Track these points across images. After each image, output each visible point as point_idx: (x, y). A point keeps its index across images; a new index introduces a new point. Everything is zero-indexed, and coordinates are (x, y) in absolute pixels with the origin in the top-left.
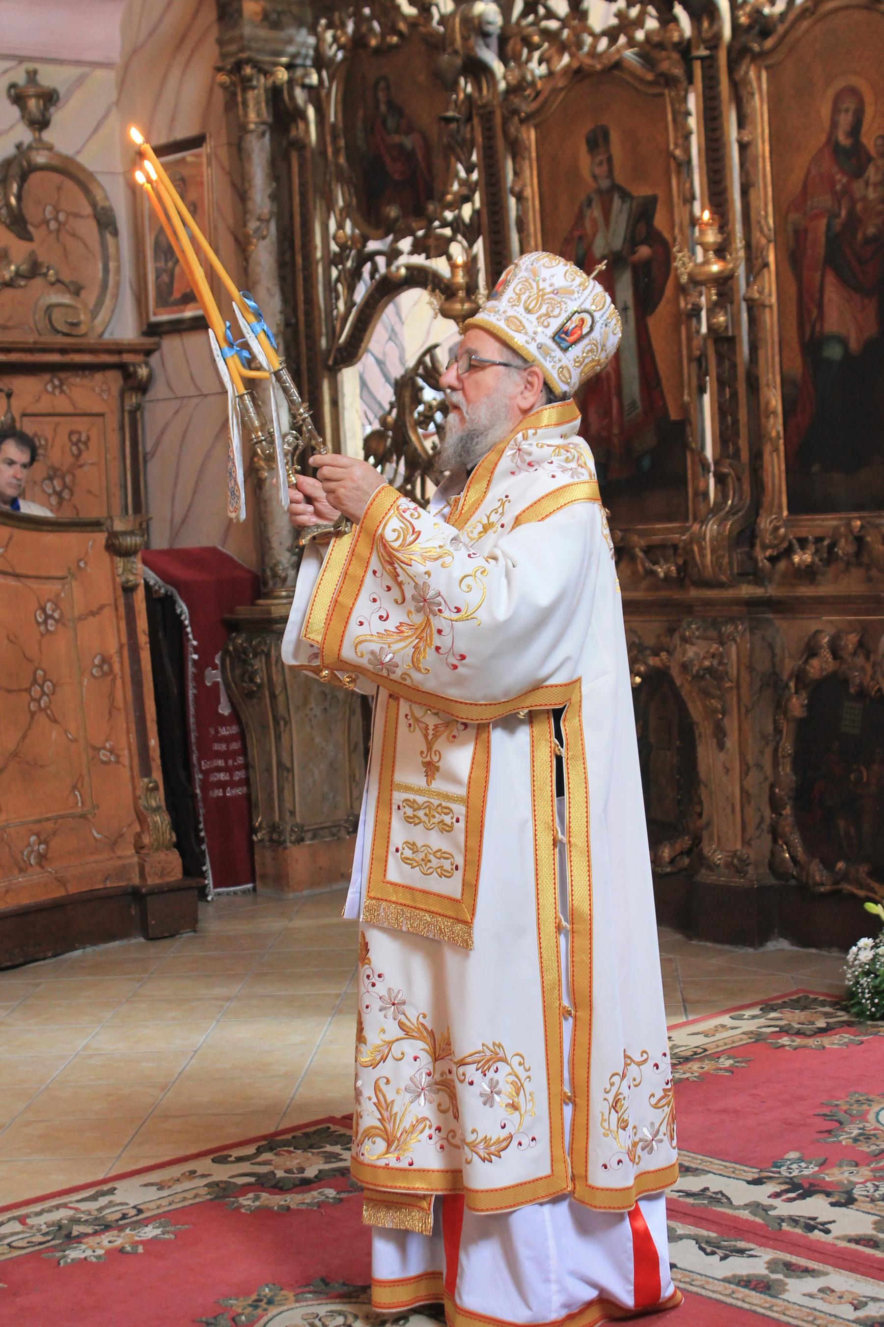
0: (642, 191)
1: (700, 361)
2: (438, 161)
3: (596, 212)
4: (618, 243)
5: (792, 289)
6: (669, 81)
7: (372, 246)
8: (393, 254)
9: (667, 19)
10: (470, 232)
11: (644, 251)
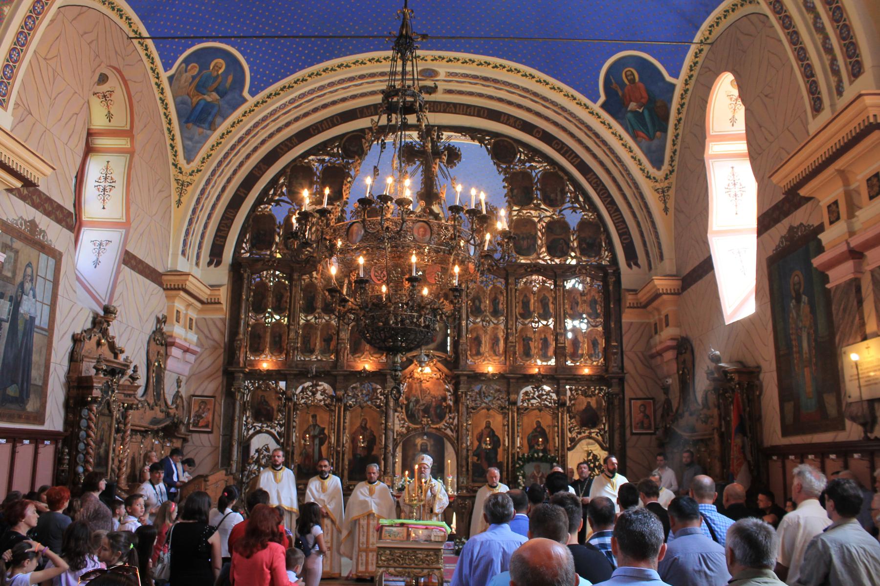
0: (323, 426)
1: (333, 455)
2: (275, 413)
3: (312, 428)
4: (316, 433)
5: (351, 446)
6: (332, 411)
7: (255, 424)
8: (262, 427)
9: (332, 401)
10: (281, 426)
11: (322, 436)
